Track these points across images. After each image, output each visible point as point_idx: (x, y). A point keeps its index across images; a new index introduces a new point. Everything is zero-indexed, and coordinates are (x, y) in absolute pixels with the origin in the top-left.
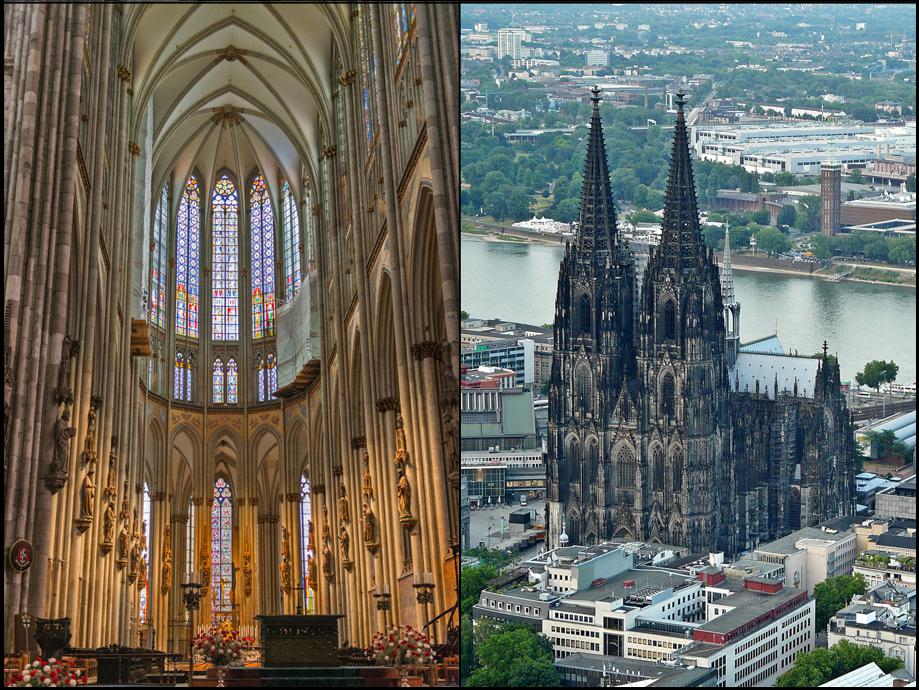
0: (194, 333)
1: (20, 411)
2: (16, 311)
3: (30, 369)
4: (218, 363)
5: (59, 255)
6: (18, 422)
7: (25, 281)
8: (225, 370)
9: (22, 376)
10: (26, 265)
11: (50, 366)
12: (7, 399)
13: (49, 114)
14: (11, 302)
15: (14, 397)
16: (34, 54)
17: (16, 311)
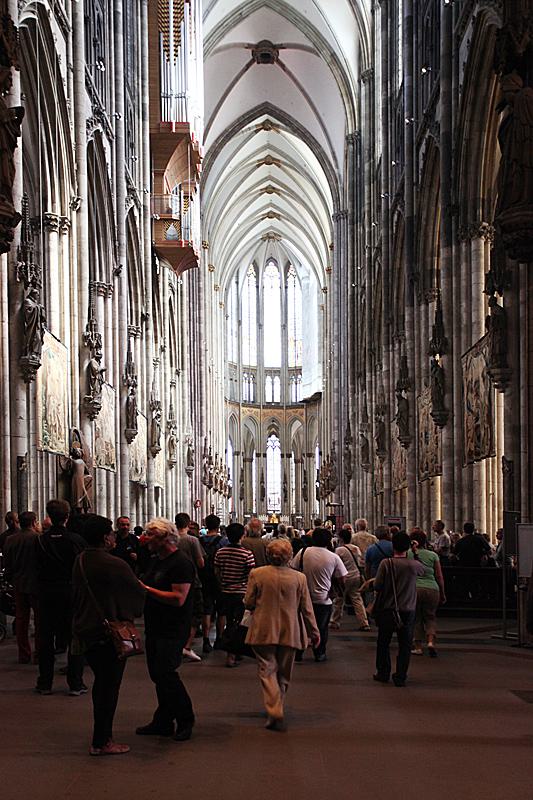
0: (254, 363)
4: (269, 379)
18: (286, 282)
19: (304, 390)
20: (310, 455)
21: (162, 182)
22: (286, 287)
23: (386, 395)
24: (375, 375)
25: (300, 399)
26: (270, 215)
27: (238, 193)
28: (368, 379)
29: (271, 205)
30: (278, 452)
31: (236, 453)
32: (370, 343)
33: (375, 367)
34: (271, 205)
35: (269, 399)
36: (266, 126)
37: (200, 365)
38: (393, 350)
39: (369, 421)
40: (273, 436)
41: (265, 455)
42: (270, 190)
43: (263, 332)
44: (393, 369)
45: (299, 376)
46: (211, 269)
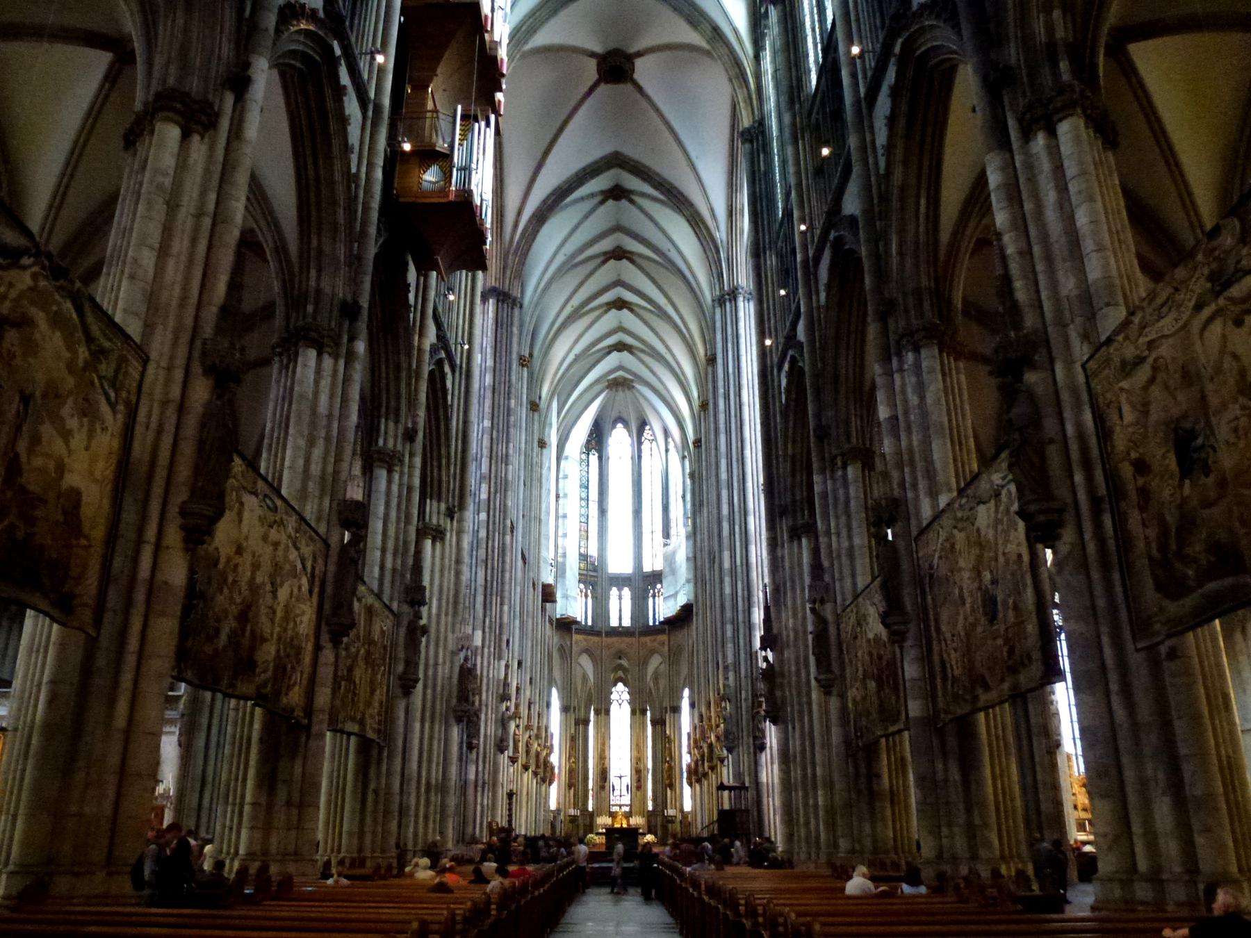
1: (484, 708)
2: (479, 651)
3: (488, 684)
5: (501, 611)
6: (483, 717)
7: (484, 632)
8: (620, 598)
9: (484, 688)
10: (484, 622)
11: (499, 680)
12: (477, 703)
13: (494, 523)
14: (477, 648)
15: (480, 701)
16: (484, 487)
17: (479, 651)
18: (640, 451)
19: (664, 607)
20: (676, 710)
21: (425, 99)
22: (640, 457)
23: (895, 475)
24: (832, 478)
25: (661, 617)
26: (620, 347)
27: (575, 302)
28: (817, 488)
29: (620, 329)
30: (627, 709)
31: (565, 709)
32: (818, 416)
33: (833, 459)
34: (620, 329)
35: (614, 623)
36: (617, 193)
37: (504, 534)
38: (901, 370)
39: (827, 578)
40: (620, 686)
41: (608, 712)
42: (620, 304)
43: (606, 520)
44: (906, 412)
45: (659, 586)
46: (534, 407)
